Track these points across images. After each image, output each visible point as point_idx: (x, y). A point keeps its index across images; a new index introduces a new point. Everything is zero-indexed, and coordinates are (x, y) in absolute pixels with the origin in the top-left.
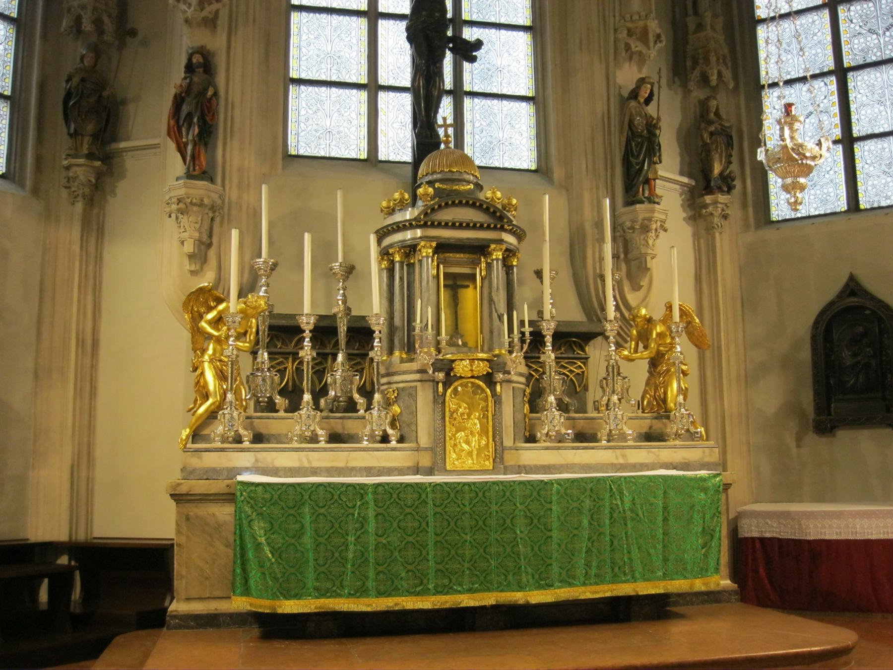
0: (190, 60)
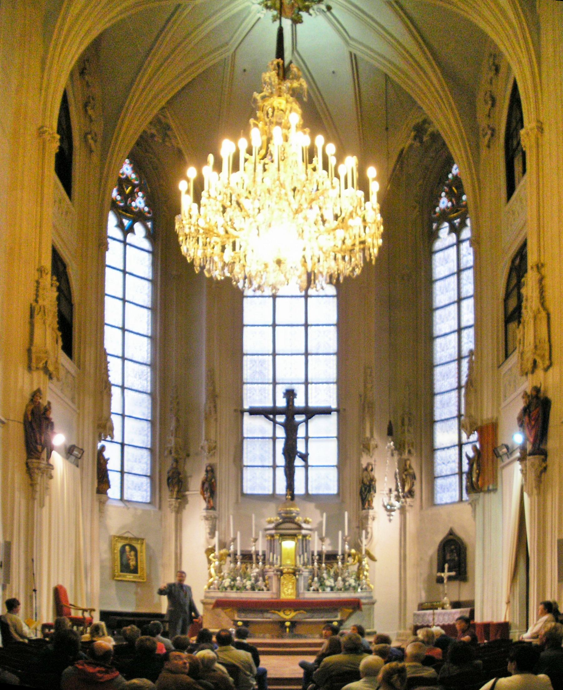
0: (207, 467)
